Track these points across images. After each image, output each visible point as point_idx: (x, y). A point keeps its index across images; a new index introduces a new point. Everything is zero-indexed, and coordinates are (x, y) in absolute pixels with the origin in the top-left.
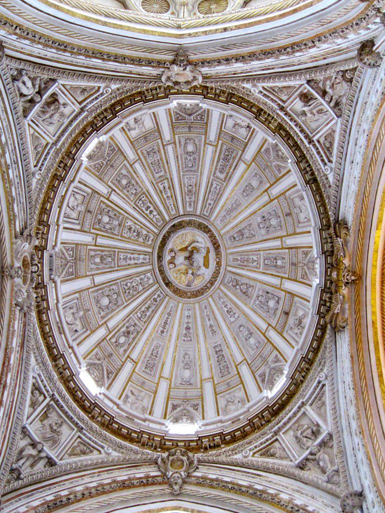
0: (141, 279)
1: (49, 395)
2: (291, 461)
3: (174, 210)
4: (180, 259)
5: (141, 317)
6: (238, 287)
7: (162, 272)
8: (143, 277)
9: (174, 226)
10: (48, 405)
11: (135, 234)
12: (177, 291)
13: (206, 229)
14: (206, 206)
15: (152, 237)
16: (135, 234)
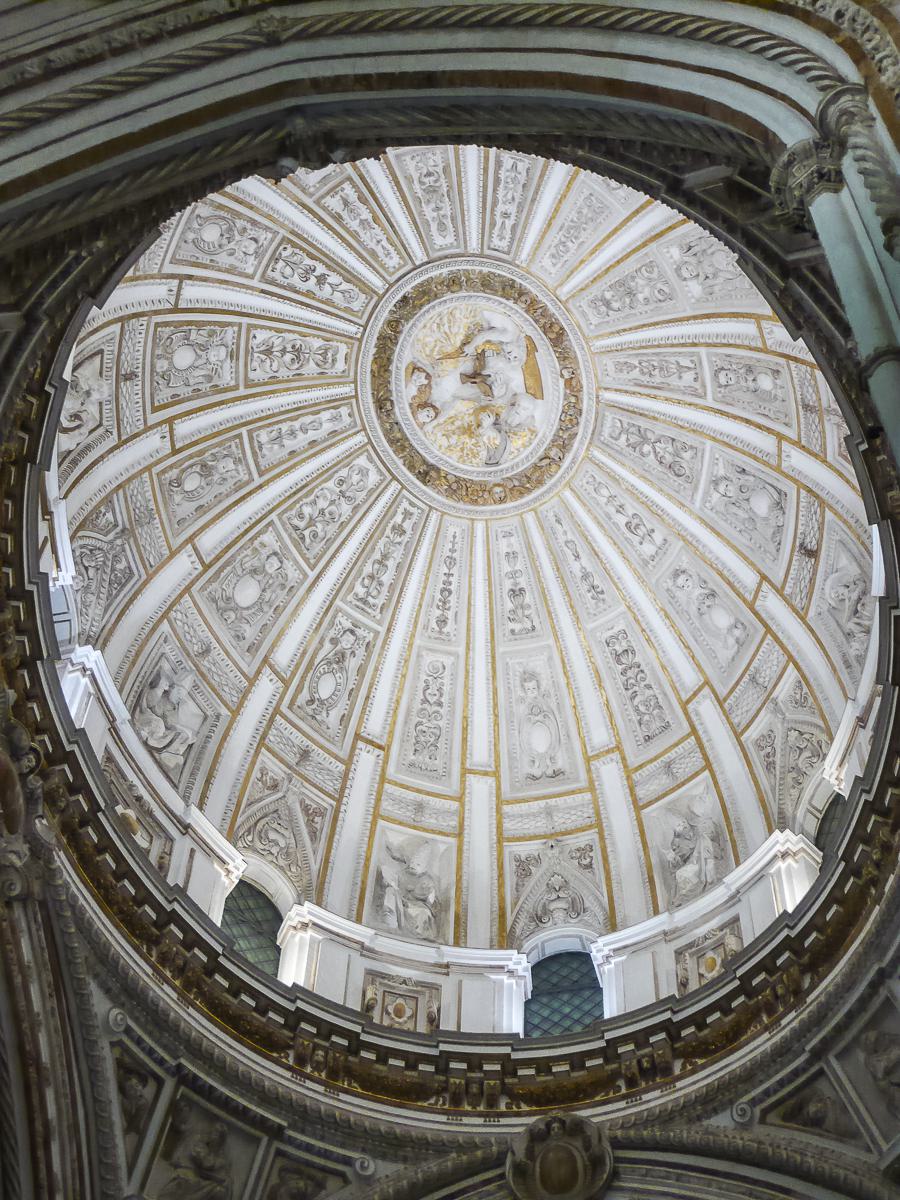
0: (341, 482)
1: (167, 1070)
2: (869, 1150)
3: (394, 253)
4: (449, 386)
5: (368, 594)
6: (647, 448)
7: (400, 443)
8: (344, 473)
9: (405, 299)
10: (174, 1108)
11: (288, 357)
12: (462, 489)
13: (510, 290)
14: (493, 224)
15: (343, 349)
16: (288, 357)
